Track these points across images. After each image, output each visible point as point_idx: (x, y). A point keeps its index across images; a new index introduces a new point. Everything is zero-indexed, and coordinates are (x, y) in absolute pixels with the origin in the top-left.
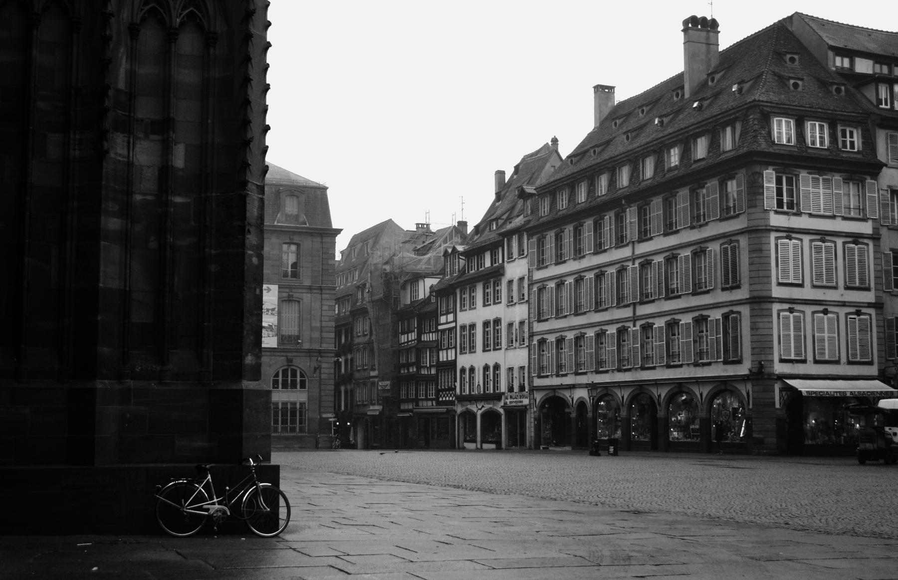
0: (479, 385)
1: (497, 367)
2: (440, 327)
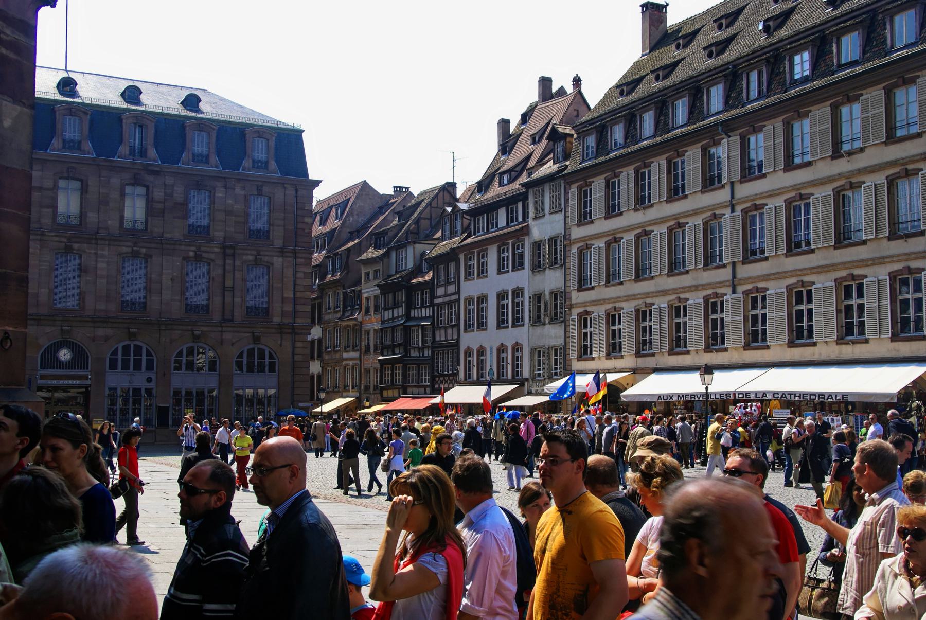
0: (491, 370)
1: (517, 348)
2: (437, 301)
